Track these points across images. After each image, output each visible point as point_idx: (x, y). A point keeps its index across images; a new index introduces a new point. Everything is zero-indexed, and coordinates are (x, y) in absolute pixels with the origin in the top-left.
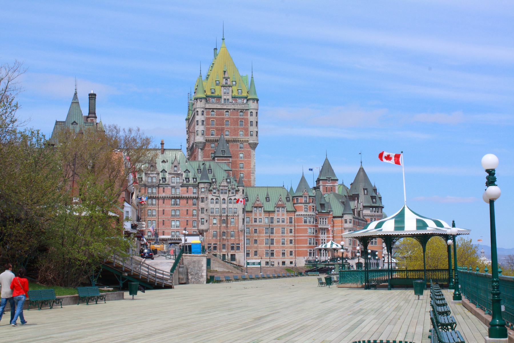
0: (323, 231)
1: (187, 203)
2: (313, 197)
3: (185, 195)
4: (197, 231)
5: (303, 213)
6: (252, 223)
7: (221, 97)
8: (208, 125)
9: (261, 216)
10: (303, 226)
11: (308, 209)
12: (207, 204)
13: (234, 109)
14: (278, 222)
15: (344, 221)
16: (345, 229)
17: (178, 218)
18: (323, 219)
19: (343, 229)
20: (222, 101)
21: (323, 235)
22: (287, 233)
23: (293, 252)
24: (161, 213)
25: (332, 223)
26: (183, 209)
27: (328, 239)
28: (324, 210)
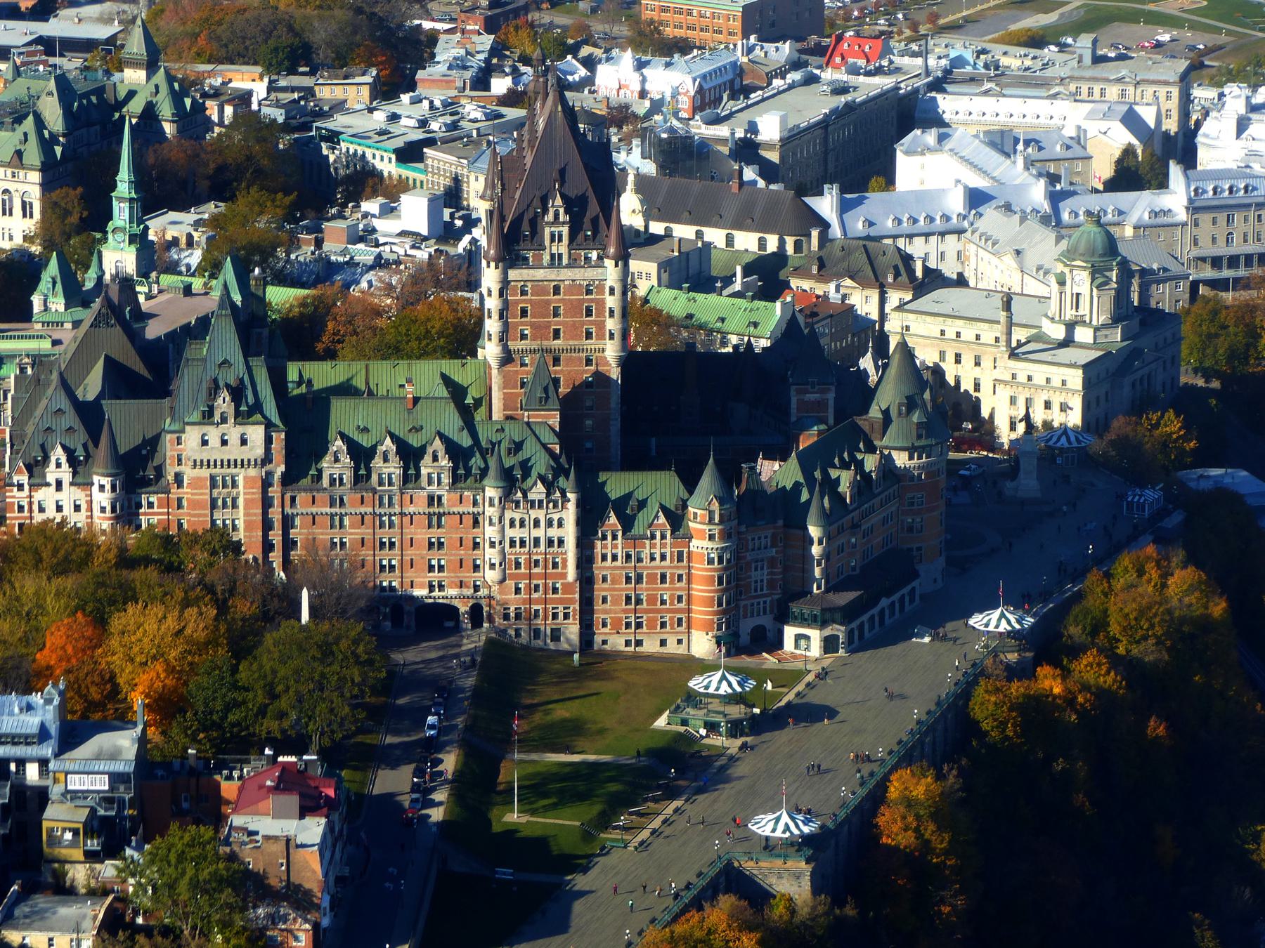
0: (759, 564)
3: (455, 510)
13: (573, 281)
14: (653, 559)
21: (759, 572)
22: (672, 582)
24: (407, 543)
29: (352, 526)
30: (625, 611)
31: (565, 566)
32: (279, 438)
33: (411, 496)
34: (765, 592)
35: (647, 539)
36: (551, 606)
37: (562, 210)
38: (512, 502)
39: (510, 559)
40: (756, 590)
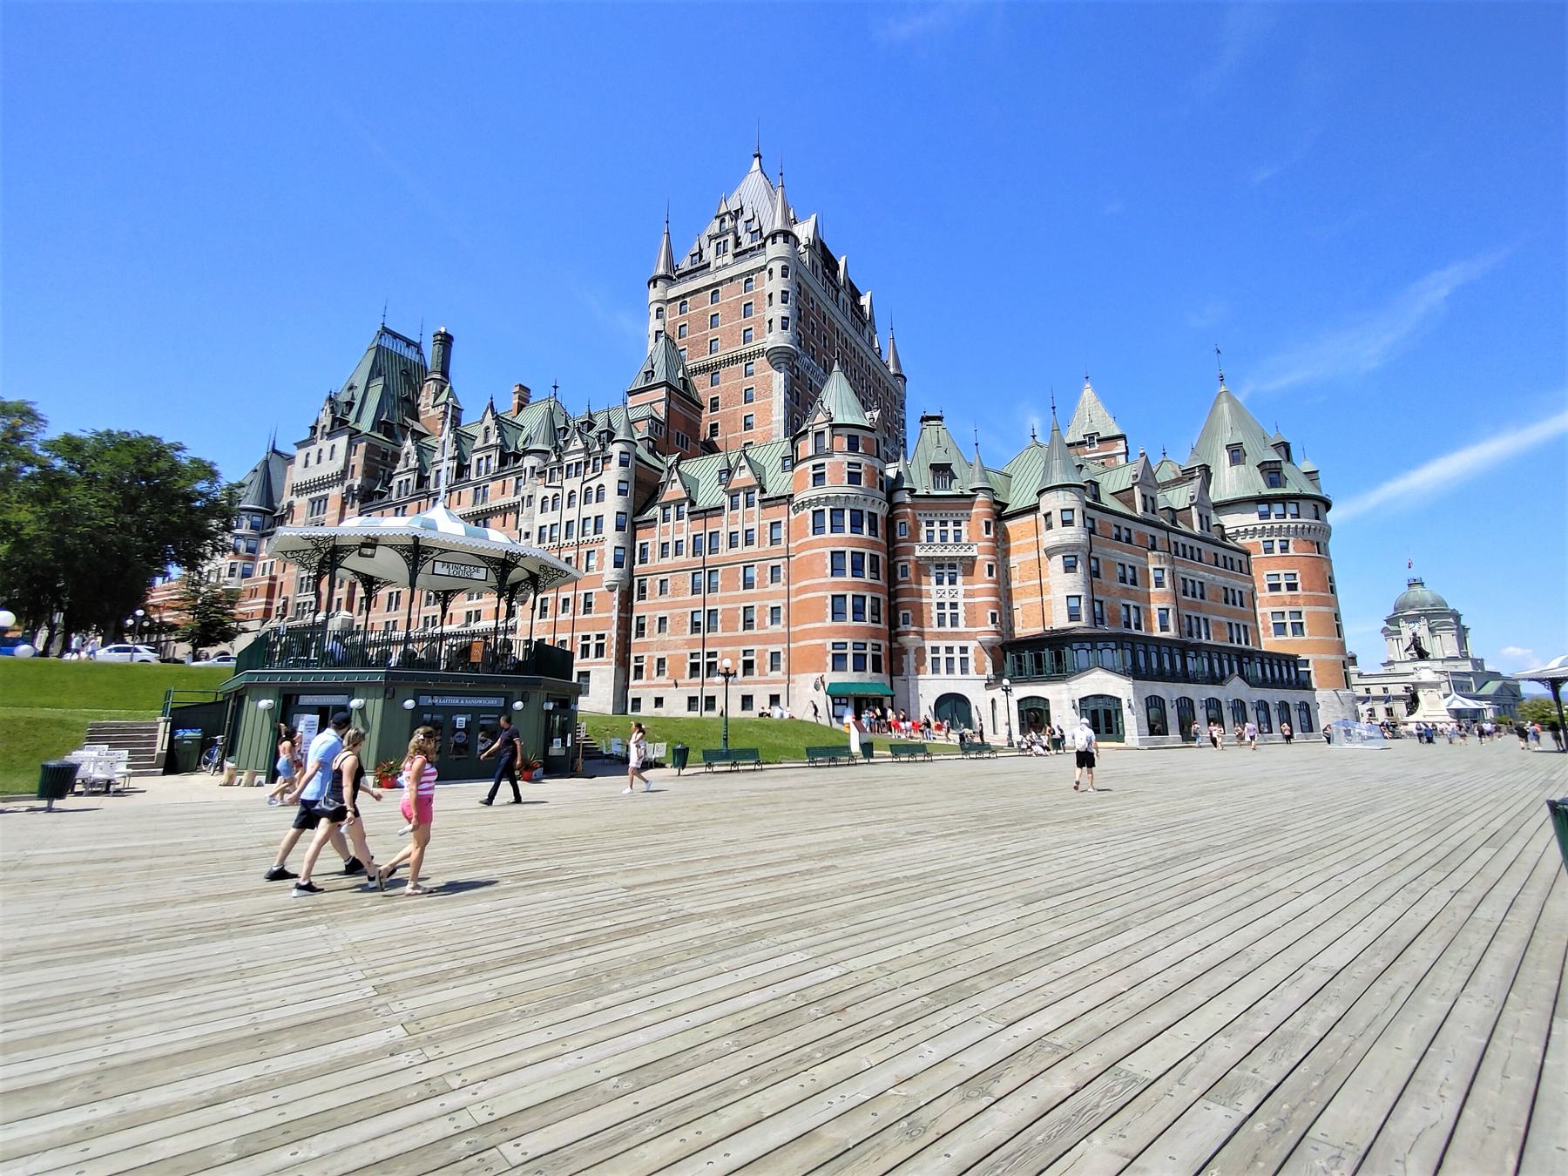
0: (946, 571)
5: (809, 492)
6: (653, 560)
7: (709, 264)
10: (810, 545)
12: (531, 517)
13: (731, 279)
14: (732, 544)
16: (1050, 553)
18: (943, 523)
19: (1043, 554)
20: (712, 268)
21: (946, 585)
23: (783, 656)
25: (992, 535)
28: (950, 489)
30: (689, 643)
36: (579, 635)
40: (941, 623)
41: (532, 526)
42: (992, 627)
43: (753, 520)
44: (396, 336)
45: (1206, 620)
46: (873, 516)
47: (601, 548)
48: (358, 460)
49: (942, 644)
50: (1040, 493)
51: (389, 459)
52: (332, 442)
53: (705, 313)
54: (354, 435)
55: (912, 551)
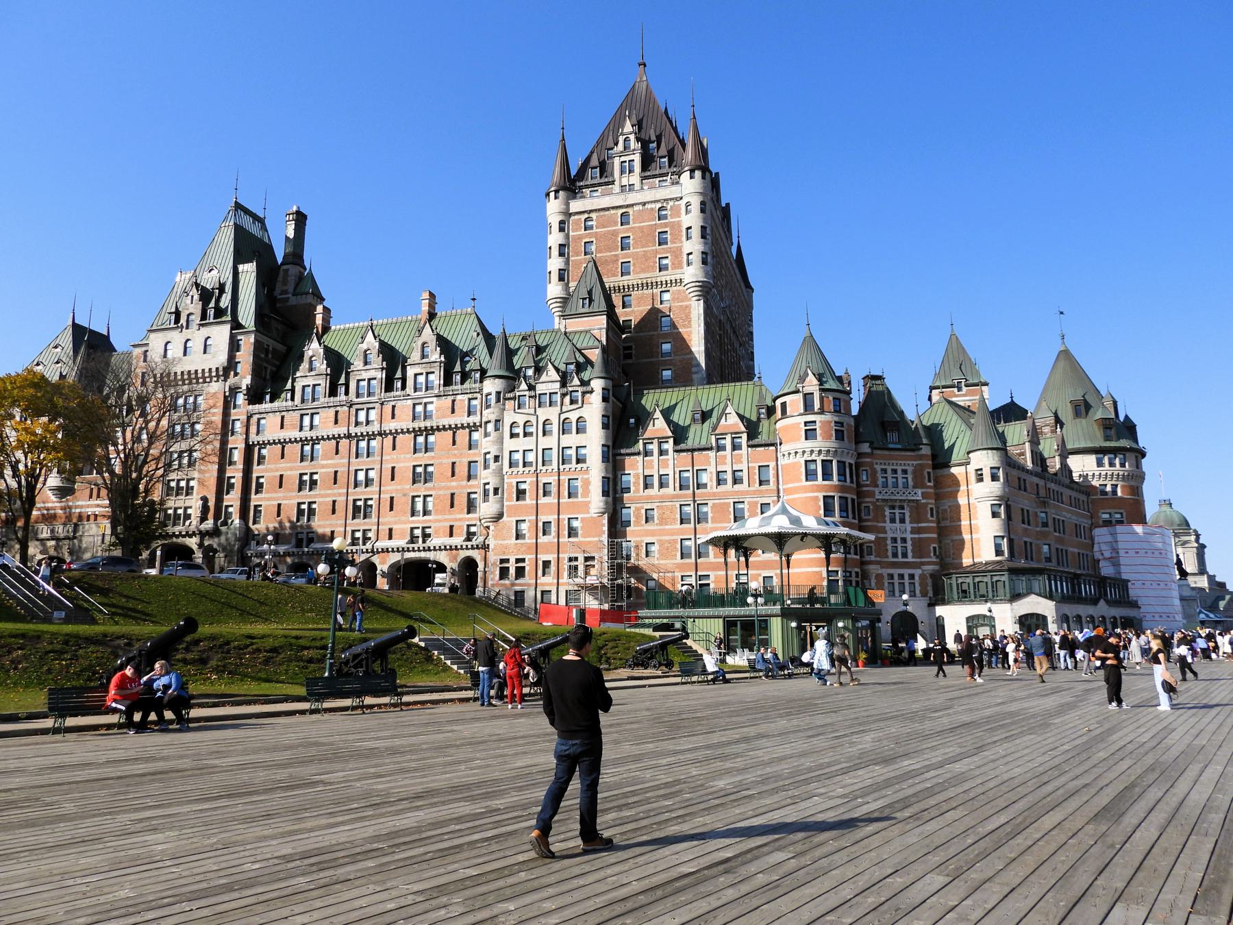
0: (897, 511)
1: (454, 443)
2: (838, 395)
4: (478, 523)
6: (637, 491)
8: (577, 254)
9: (667, 466)
11: (818, 432)
12: (500, 441)
13: (644, 204)
14: (720, 482)
15: (972, 477)
17: (430, 489)
21: (898, 525)
24: (387, 474)
26: (444, 461)
27: (916, 536)
29: (325, 457)
30: (680, 567)
31: (587, 492)
32: (247, 343)
33: (394, 407)
34: (910, 559)
35: (711, 449)
37: (632, 137)
38: (514, 398)
39: (510, 484)
40: (895, 555)
41: (502, 450)
42: (934, 559)
43: (741, 462)
44: (247, 212)
45: (1066, 551)
46: (850, 465)
47: (586, 476)
48: (245, 357)
49: (896, 572)
50: (969, 453)
51: (270, 356)
52: (205, 331)
53: (615, 233)
54: (236, 325)
55: (872, 494)
